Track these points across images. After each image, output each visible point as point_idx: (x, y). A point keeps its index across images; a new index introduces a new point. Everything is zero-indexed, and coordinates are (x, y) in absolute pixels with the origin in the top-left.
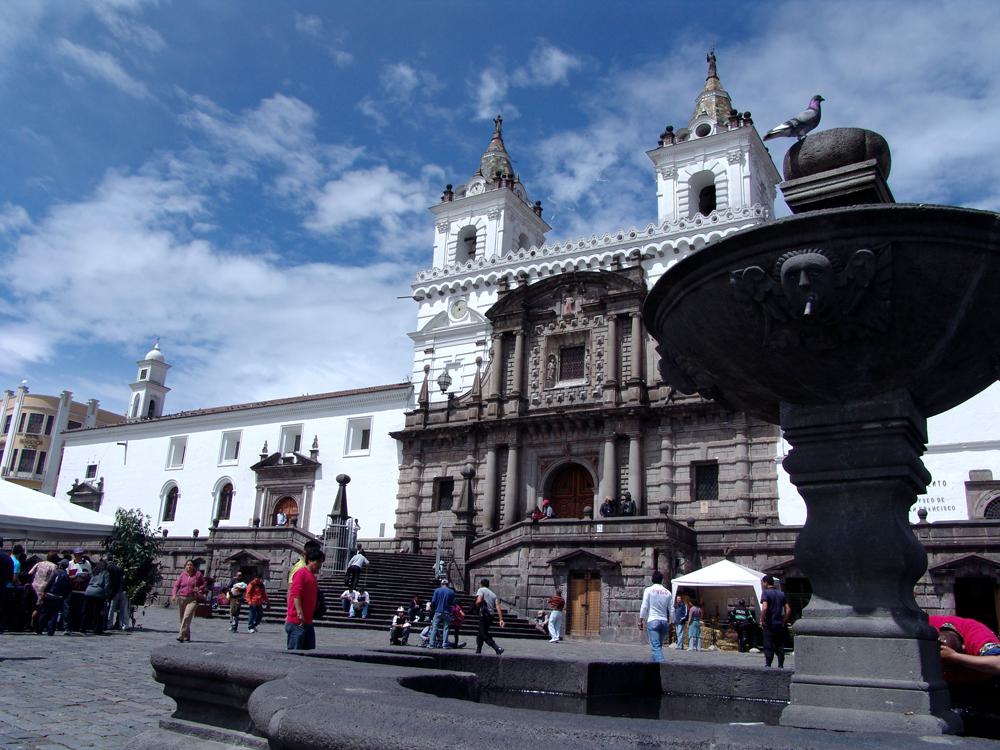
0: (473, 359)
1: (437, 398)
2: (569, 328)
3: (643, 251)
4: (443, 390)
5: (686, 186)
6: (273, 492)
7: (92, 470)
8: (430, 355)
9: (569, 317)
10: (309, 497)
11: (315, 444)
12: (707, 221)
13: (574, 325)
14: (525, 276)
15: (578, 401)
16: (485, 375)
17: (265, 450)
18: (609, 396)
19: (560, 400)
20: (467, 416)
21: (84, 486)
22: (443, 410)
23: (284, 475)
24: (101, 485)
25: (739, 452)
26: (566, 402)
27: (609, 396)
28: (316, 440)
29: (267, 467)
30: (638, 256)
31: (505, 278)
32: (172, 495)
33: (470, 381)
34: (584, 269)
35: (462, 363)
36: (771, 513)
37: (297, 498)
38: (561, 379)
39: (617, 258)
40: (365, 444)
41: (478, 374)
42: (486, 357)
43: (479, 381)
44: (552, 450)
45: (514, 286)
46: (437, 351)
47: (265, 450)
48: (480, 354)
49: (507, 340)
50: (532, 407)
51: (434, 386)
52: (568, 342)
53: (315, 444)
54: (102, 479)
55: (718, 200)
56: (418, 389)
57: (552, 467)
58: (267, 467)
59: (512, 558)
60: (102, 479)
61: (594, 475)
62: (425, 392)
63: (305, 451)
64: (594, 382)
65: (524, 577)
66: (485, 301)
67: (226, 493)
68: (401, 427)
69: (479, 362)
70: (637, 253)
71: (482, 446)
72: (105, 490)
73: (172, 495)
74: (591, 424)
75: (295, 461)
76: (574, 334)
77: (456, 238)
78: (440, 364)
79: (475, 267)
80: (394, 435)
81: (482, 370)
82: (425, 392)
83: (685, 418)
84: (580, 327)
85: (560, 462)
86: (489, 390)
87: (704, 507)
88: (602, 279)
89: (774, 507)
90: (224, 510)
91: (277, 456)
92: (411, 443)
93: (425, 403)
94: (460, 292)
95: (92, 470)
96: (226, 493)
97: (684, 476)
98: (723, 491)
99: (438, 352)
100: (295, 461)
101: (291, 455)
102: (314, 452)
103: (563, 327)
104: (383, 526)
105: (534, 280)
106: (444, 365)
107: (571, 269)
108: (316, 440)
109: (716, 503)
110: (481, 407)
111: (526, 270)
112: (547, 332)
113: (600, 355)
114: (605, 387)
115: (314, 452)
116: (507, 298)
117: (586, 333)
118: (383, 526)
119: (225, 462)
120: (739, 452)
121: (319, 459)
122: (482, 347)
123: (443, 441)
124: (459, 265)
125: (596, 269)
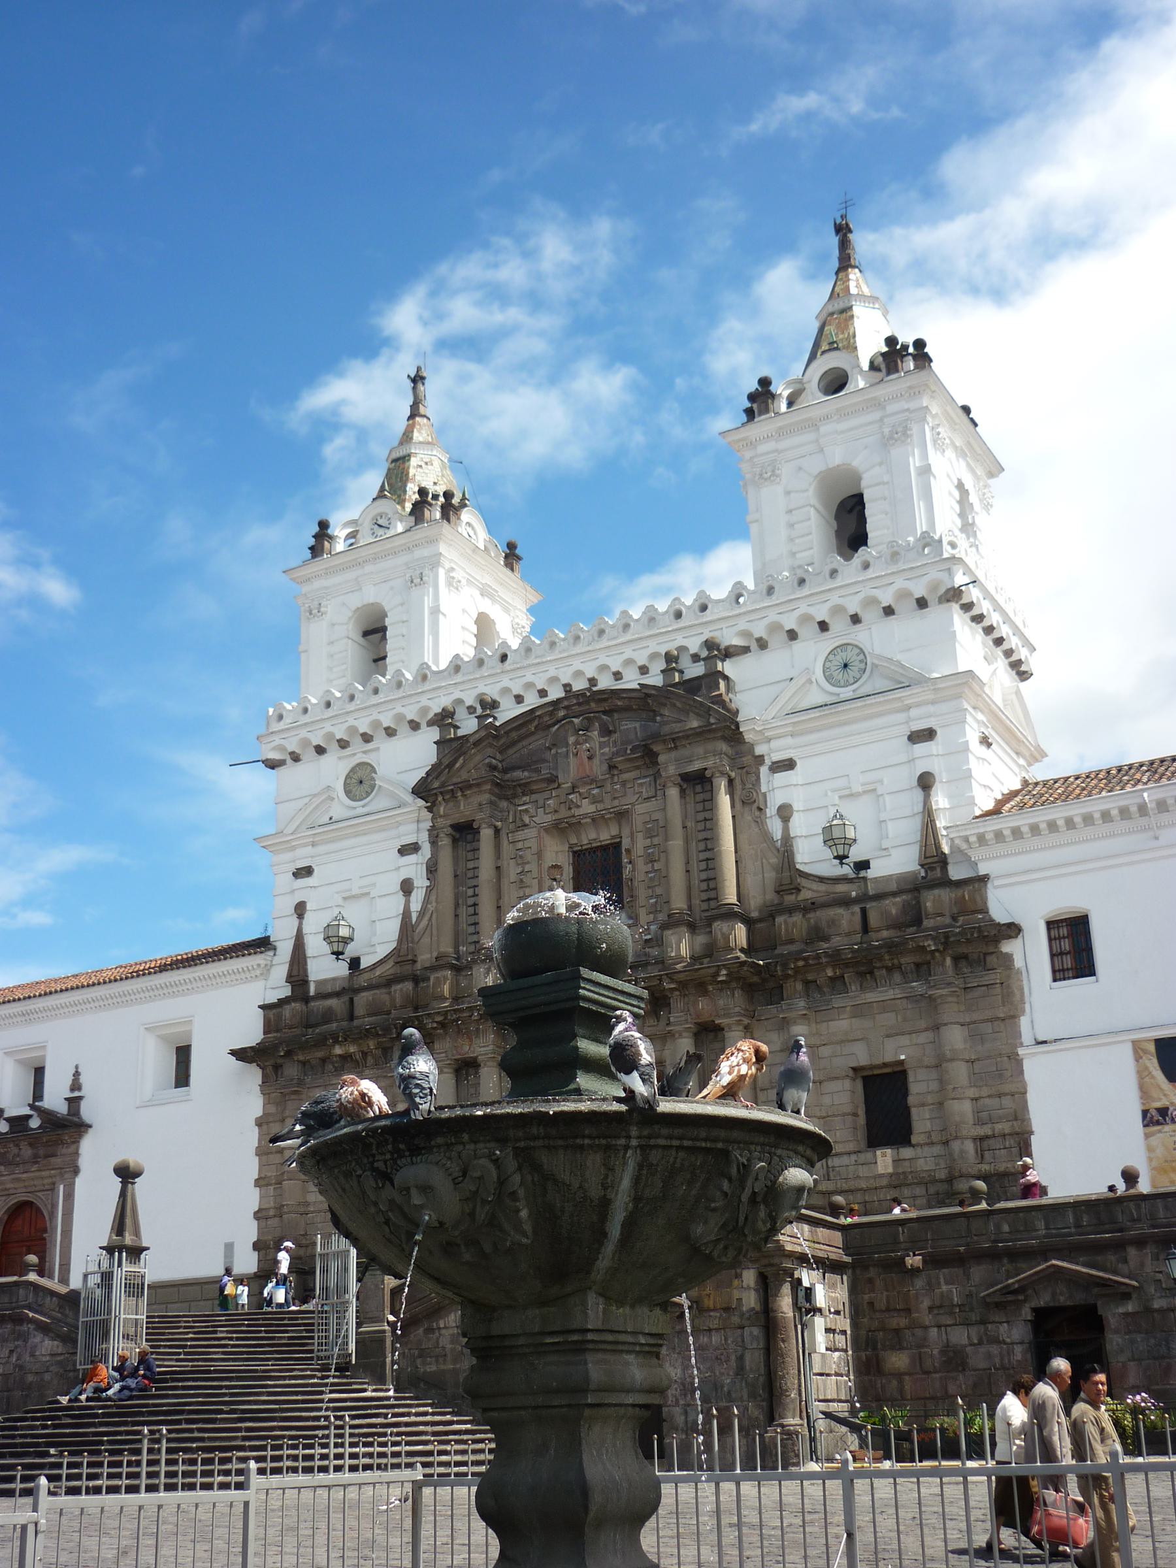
1: (324, 968)
3: (730, 638)
4: (338, 954)
10: (69, 1196)
11: (76, 1086)
14: (489, 705)
16: (422, 914)
18: (682, 946)
22: (337, 994)
28: (77, 1074)
30: (716, 651)
37: (40, 1200)
39: (669, 658)
40: (182, 1078)
41: (406, 914)
42: (421, 882)
45: (468, 725)
49: (464, 832)
51: (316, 946)
53: (76, 1086)
56: (285, 949)
63: (55, 1098)
66: (411, 757)
69: (407, 887)
70: (710, 645)
76: (597, 820)
80: (240, 1054)
87: (885, 1160)
88: (643, 701)
92: (277, 1068)
94: (357, 745)
98: (922, 1122)
100: (35, 1123)
102: (74, 1102)
104: (229, 1248)
105: (508, 712)
108: (77, 1074)
109: (907, 1152)
111: (492, 692)
115: (74, 1102)
116: (452, 748)
117: (622, 816)
118: (229, 1248)
121: (87, 1112)
122: (412, 858)
123: (346, 1058)
125: (632, 681)
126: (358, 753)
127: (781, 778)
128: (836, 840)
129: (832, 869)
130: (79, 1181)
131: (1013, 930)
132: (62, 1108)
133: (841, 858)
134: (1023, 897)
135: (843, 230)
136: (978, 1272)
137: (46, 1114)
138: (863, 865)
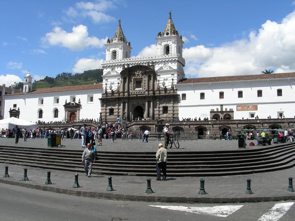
0: (117, 82)
1: (109, 91)
2: (138, 77)
3: (154, 61)
5: (163, 47)
6: (69, 111)
7: (15, 106)
8: (107, 81)
9: (138, 75)
10: (79, 112)
11: (79, 100)
12: (167, 57)
13: (139, 76)
14: (128, 65)
15: (140, 93)
16: (120, 86)
17: (66, 101)
19: (137, 93)
20: (116, 95)
21: (14, 110)
22: (111, 94)
23: (73, 109)
24: (19, 109)
25: (172, 105)
26: (138, 93)
27: (147, 93)
28: (79, 99)
29: (67, 106)
30: (153, 63)
31: (124, 65)
32: (41, 112)
33: (117, 87)
34: (142, 64)
35: (114, 83)
36: (177, 116)
37: (76, 113)
38: (136, 88)
39: (148, 63)
41: (118, 86)
42: (120, 82)
43: (119, 88)
44: (135, 103)
45: (126, 67)
46: (108, 80)
47: (66, 101)
48: (119, 82)
50: (130, 94)
51: (108, 88)
52: (138, 80)
53: (79, 100)
54: (19, 108)
55: (170, 50)
56: (104, 88)
57: (135, 106)
58: (67, 106)
59: (133, 127)
60: (19, 108)
61: (144, 108)
62: (106, 89)
64: (144, 89)
65: (135, 130)
66: (119, 70)
67: (56, 112)
68: (101, 97)
69: (118, 83)
70: (153, 62)
71: (120, 102)
72: (20, 111)
73: (41, 112)
74: (143, 98)
75: (75, 104)
77: (111, 53)
78: (109, 83)
79: (117, 61)
81: (119, 85)
82: (106, 89)
83: (162, 98)
84: (141, 77)
85: (136, 105)
86: (121, 90)
87: (165, 115)
89: (178, 115)
90: (56, 115)
91: (70, 103)
93: (106, 92)
95: (15, 106)
96: (56, 112)
97: (161, 109)
98: (169, 112)
99: (109, 80)
101: (73, 103)
102: (79, 102)
103: (137, 77)
105: (131, 66)
106: (110, 83)
107: (138, 64)
108: (79, 99)
110: (119, 93)
111: (129, 63)
112: (133, 78)
113: (145, 83)
114: (146, 91)
115: (79, 102)
117: (142, 78)
119: (55, 104)
120: (172, 105)
121: (81, 104)
122: (119, 80)
124: (113, 60)
126: (113, 67)
127: (159, 77)
128: (164, 84)
129: (162, 87)
130: (80, 112)
131: (179, 95)
132: (78, 103)
133: (164, 86)
134: (180, 93)
135: (170, 14)
136: (172, 126)
137: (76, 104)
138: (166, 87)
